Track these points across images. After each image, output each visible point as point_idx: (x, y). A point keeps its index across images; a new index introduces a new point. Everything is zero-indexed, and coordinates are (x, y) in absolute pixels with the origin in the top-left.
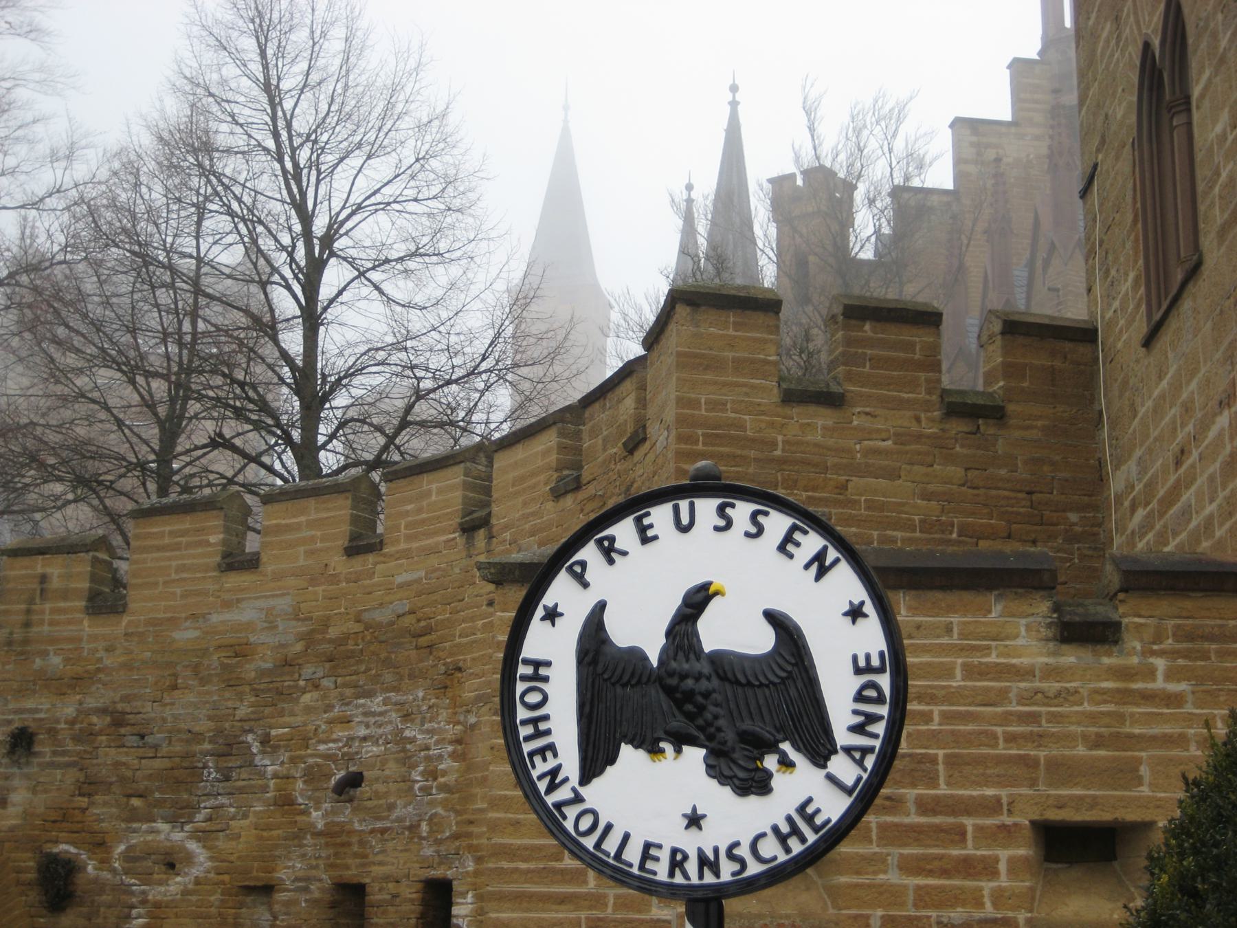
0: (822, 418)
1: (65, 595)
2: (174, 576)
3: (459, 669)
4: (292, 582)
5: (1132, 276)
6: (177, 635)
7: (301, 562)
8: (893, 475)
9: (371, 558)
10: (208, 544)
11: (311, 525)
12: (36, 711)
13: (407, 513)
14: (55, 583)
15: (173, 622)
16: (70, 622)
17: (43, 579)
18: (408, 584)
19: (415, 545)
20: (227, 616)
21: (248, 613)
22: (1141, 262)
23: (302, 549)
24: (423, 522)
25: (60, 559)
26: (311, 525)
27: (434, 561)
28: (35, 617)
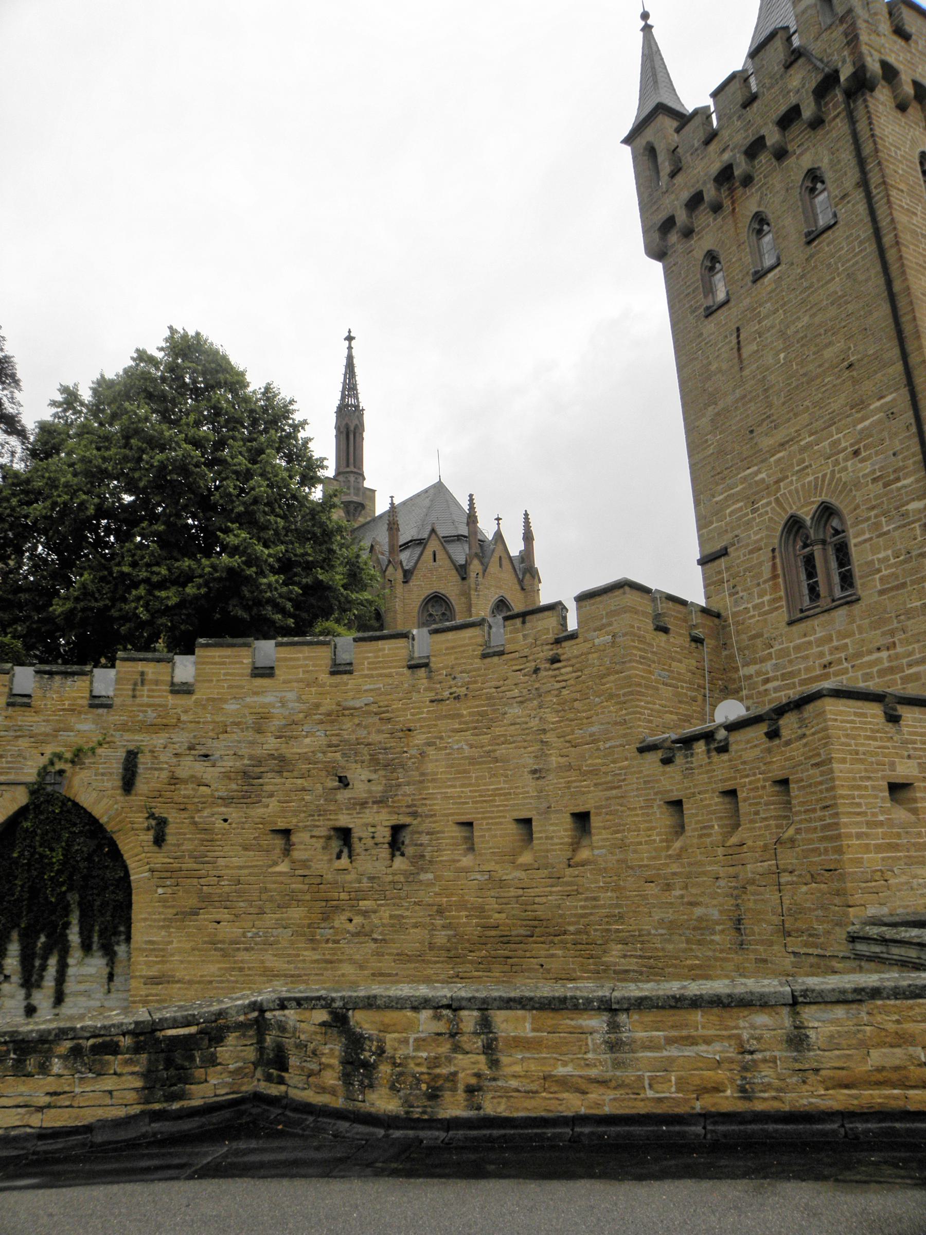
0: (662, 637)
1: (157, 682)
2: (222, 677)
3: (410, 730)
4: (295, 684)
5: (766, 598)
6: (225, 706)
7: (301, 676)
8: (680, 661)
9: (345, 677)
10: (242, 663)
11: (305, 658)
12: (142, 741)
13: (368, 658)
14: (150, 676)
15: (223, 700)
16: (159, 697)
17: (142, 674)
18: (371, 690)
19: (374, 672)
20: (256, 699)
21: (268, 699)
22: (782, 593)
23: (301, 670)
24: (380, 662)
25: (152, 664)
26: (305, 658)
27: (390, 681)
28: (138, 693)
